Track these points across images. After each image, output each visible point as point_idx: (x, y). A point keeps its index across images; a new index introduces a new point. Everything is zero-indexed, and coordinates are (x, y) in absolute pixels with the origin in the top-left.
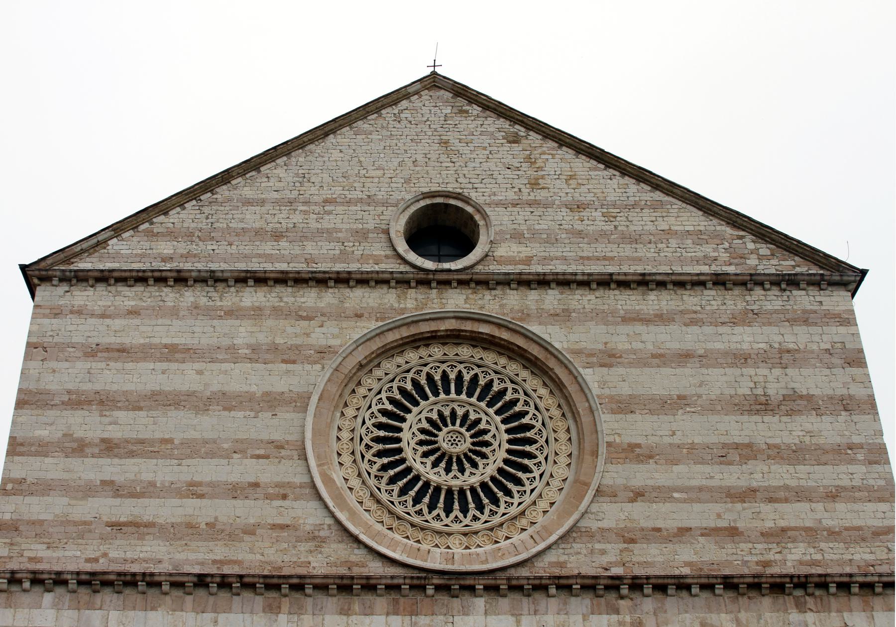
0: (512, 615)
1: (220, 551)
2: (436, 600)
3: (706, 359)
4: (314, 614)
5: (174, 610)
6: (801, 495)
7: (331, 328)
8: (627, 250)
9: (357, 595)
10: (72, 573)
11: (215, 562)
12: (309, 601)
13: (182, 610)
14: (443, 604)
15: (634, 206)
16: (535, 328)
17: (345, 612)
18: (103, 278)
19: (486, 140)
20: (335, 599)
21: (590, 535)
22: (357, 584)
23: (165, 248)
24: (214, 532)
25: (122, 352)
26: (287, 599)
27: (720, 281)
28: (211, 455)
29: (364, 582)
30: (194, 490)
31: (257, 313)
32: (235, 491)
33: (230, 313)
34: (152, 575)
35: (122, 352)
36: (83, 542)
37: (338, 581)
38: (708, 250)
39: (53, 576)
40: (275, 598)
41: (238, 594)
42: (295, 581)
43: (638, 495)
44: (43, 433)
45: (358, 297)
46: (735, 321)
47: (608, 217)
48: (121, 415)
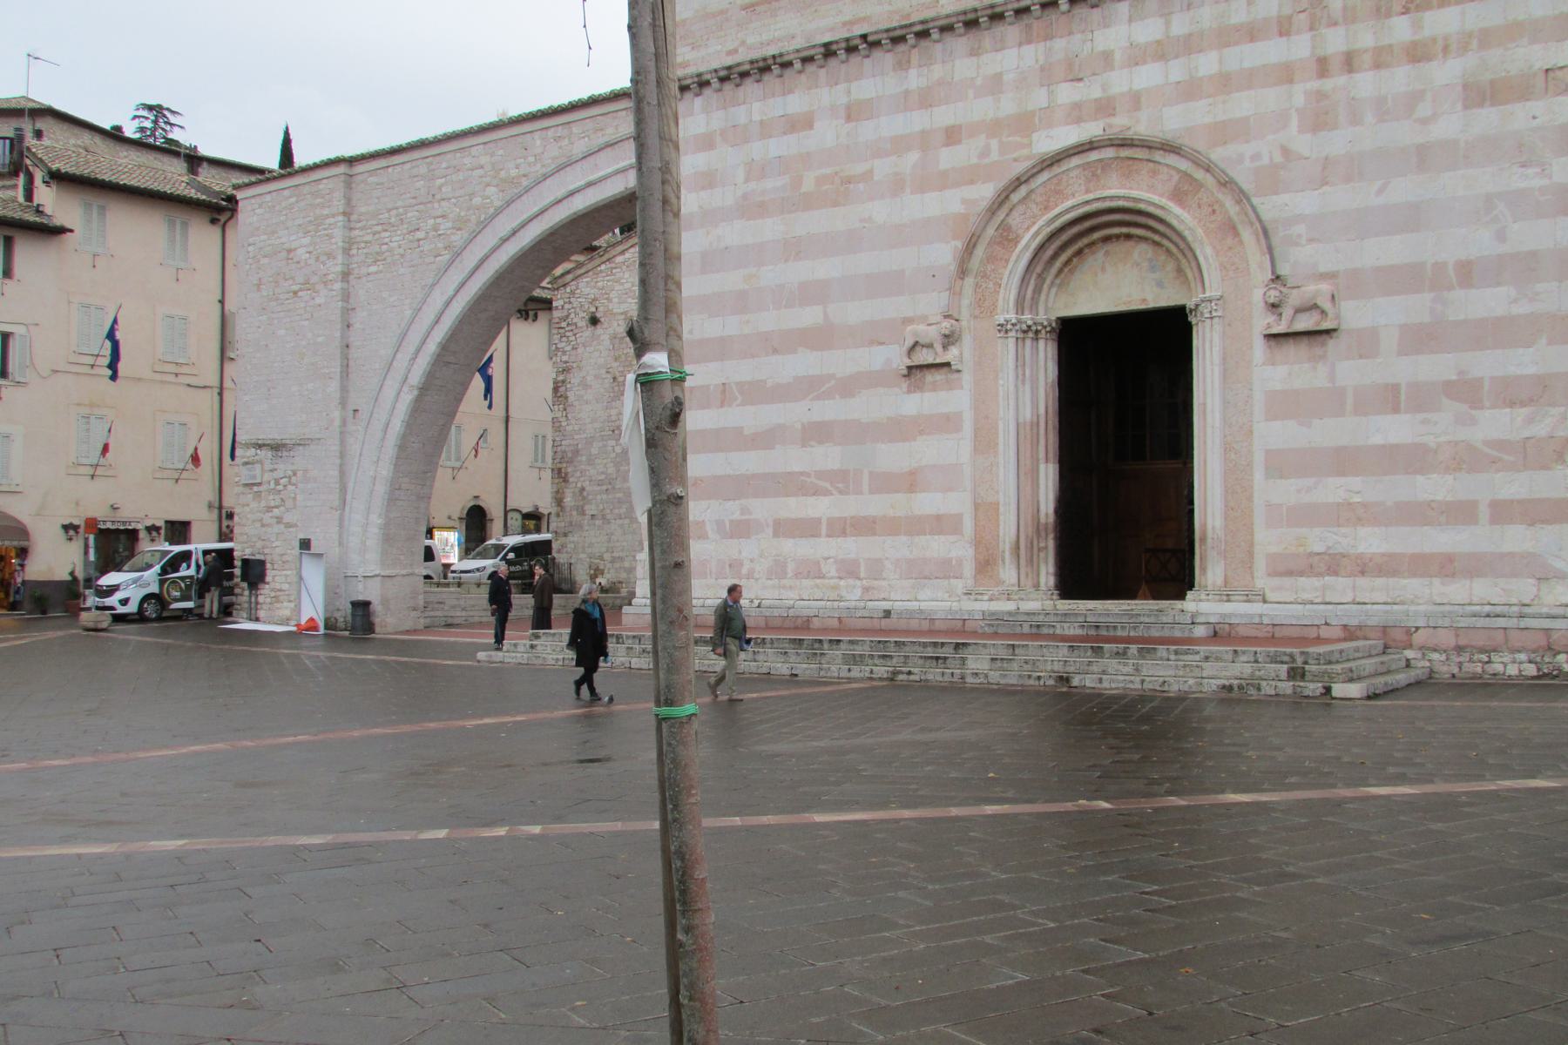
0: (1161, 16)
2: (1073, 16)
4: (943, 62)
5: (810, 88)
9: (987, 29)
10: (711, 72)
11: (845, 24)
12: (939, 46)
13: (817, 87)
14: (1081, 19)
17: (974, 52)
20: (964, 40)
22: (982, 17)
26: (916, 49)
29: (989, 12)
34: (781, 55)
36: (723, 33)
37: (962, 18)
39: (696, 79)
40: (903, 52)
41: (868, 56)
42: (918, 28)
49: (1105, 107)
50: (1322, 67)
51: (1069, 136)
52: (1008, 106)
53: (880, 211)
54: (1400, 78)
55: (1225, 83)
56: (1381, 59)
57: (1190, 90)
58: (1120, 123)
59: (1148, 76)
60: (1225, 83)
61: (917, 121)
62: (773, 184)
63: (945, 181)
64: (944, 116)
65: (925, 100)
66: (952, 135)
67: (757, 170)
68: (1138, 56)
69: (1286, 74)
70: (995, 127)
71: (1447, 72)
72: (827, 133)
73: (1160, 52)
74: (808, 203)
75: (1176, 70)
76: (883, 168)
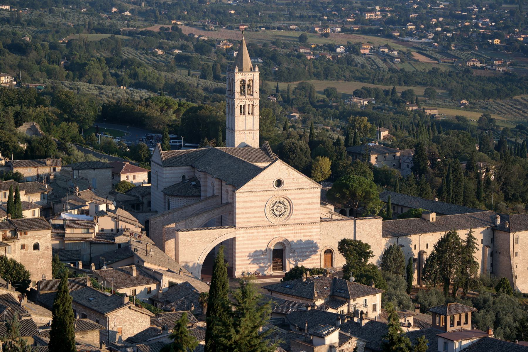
1: (258, 223)
3: (304, 198)
6: (311, 214)
7: (267, 197)
8: (298, 185)
15: (300, 178)
16: (287, 196)
18: (244, 192)
19: (284, 169)
21: (291, 219)
23: (249, 188)
24: (257, 221)
25: (246, 202)
27: (307, 189)
28: (256, 213)
30: (255, 217)
31: (260, 196)
32: (259, 217)
33: (257, 196)
35: (246, 202)
38: (306, 184)
43: (296, 215)
44: (239, 212)
45: (271, 193)
46: (308, 193)
47: (297, 180)
48: (247, 209)
49: (279, 234)
50: (295, 233)
51: (276, 236)
52: (272, 233)
53: (261, 241)
54: (300, 234)
55: (288, 234)
56: (298, 233)
57: (286, 234)
58: (280, 236)
59: (283, 232)
60: (288, 234)
61: (264, 234)
62: (250, 238)
63: (266, 239)
64: (266, 234)
65: (265, 232)
66: (267, 235)
67: (249, 236)
68: (282, 231)
69: (292, 233)
70: (271, 235)
71: (302, 234)
72: (256, 234)
73: (284, 231)
74: (254, 240)
75: (285, 232)
76: (261, 237)
